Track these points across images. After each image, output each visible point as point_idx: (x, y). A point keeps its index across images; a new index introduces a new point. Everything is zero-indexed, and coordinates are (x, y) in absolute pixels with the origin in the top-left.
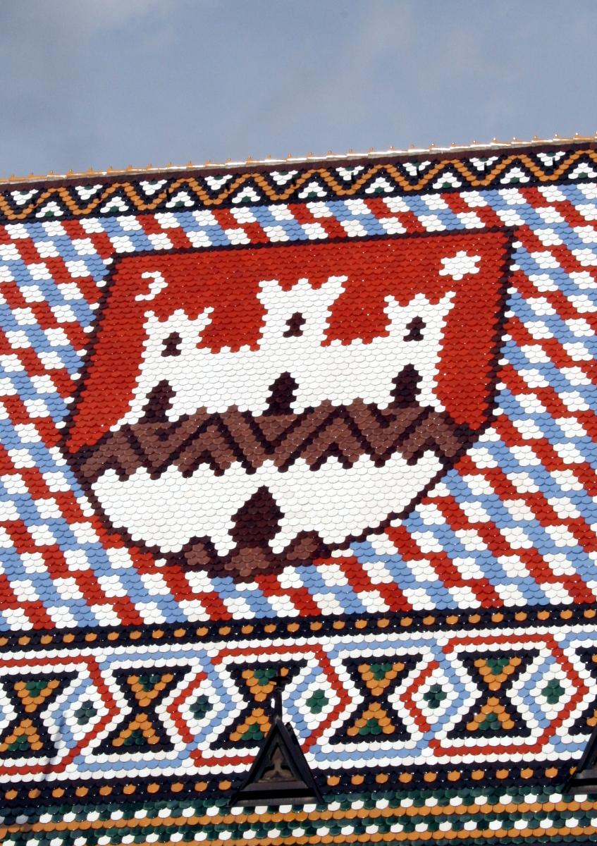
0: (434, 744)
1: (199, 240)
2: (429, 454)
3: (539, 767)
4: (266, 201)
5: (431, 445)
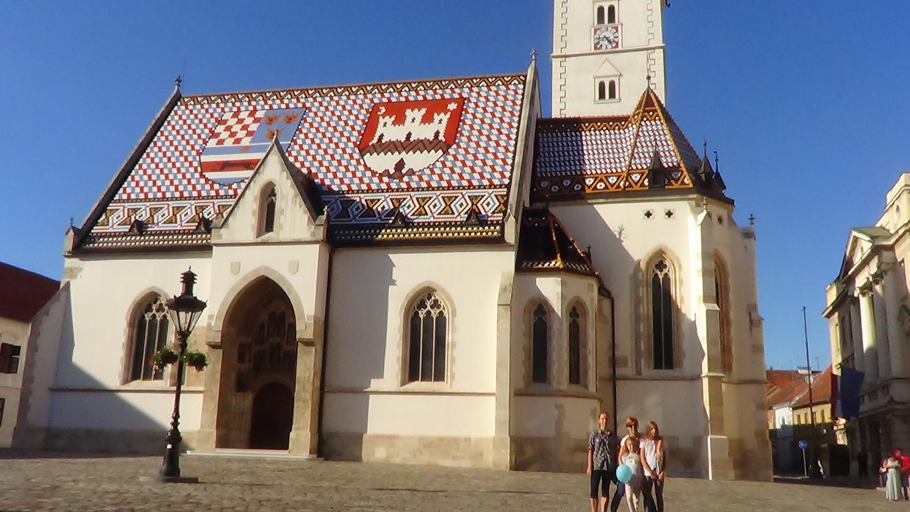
1: (394, 100)
2: (440, 150)
3: (456, 222)
5: (441, 148)
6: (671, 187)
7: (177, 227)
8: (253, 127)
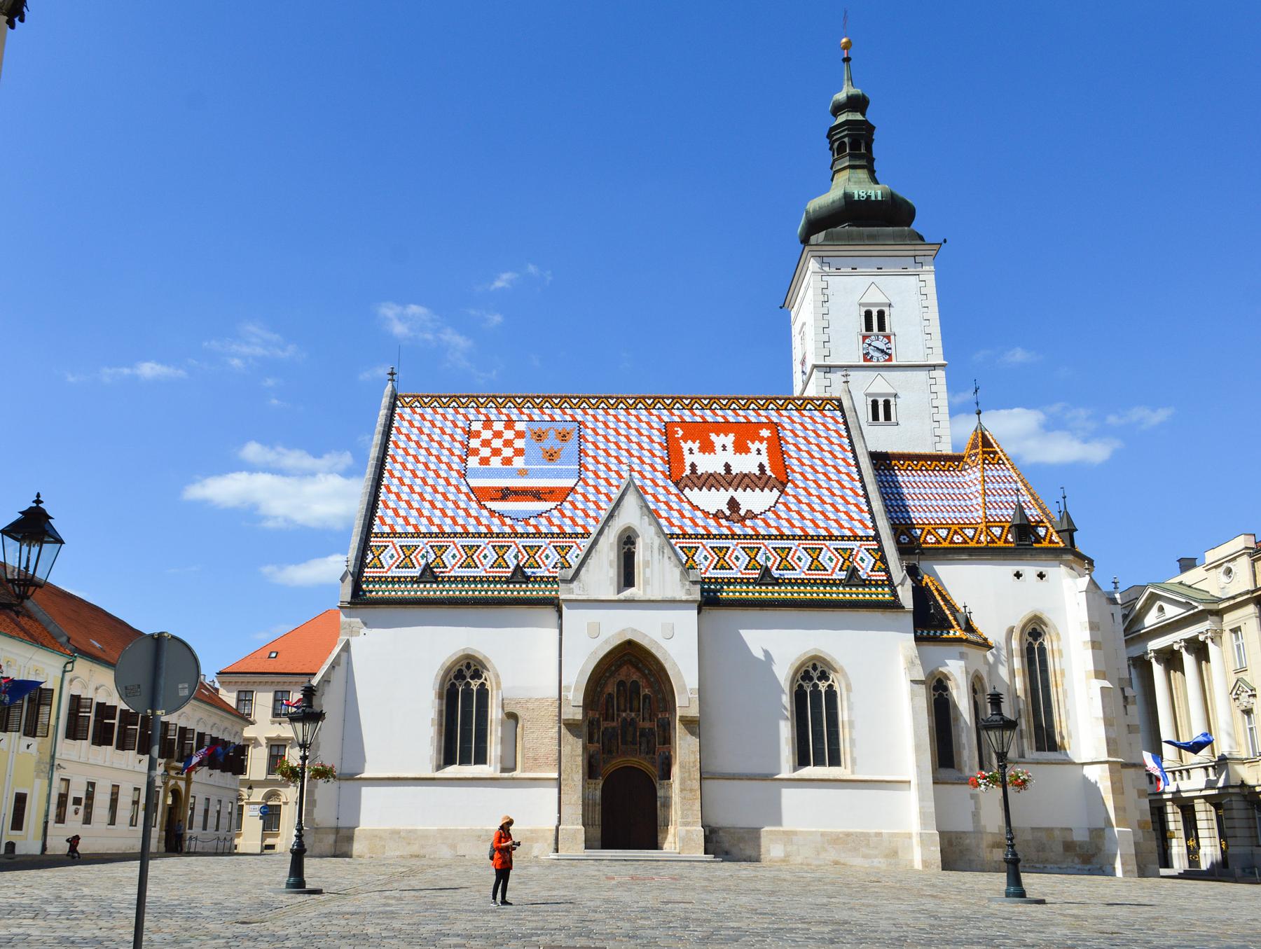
0: (804, 572)
1: (688, 419)
4: (703, 409)
6: (1039, 545)
7: (479, 572)
8: (519, 444)
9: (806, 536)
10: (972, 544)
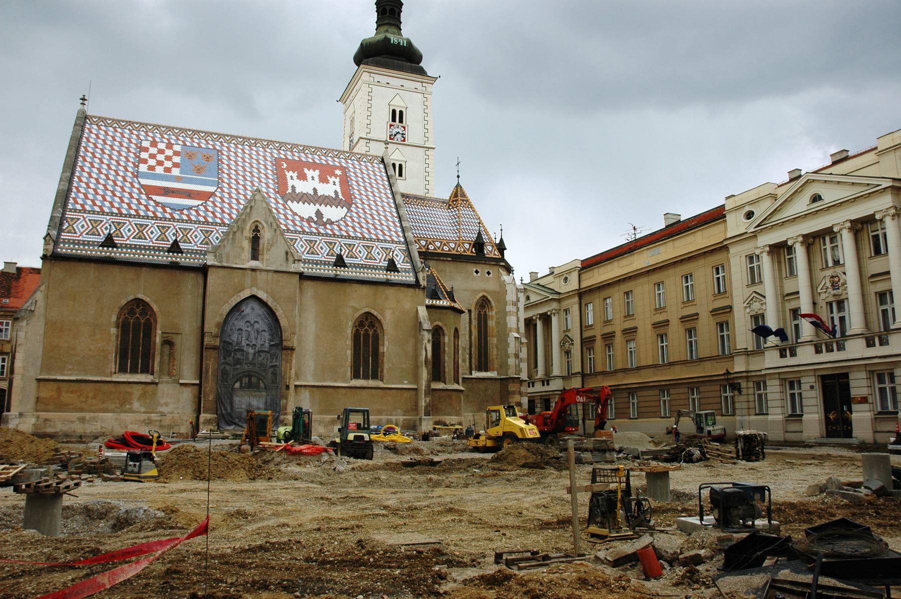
1: (290, 158)
3: (381, 266)
4: (299, 152)
8: (177, 159)
9: (364, 238)
10: (454, 252)
